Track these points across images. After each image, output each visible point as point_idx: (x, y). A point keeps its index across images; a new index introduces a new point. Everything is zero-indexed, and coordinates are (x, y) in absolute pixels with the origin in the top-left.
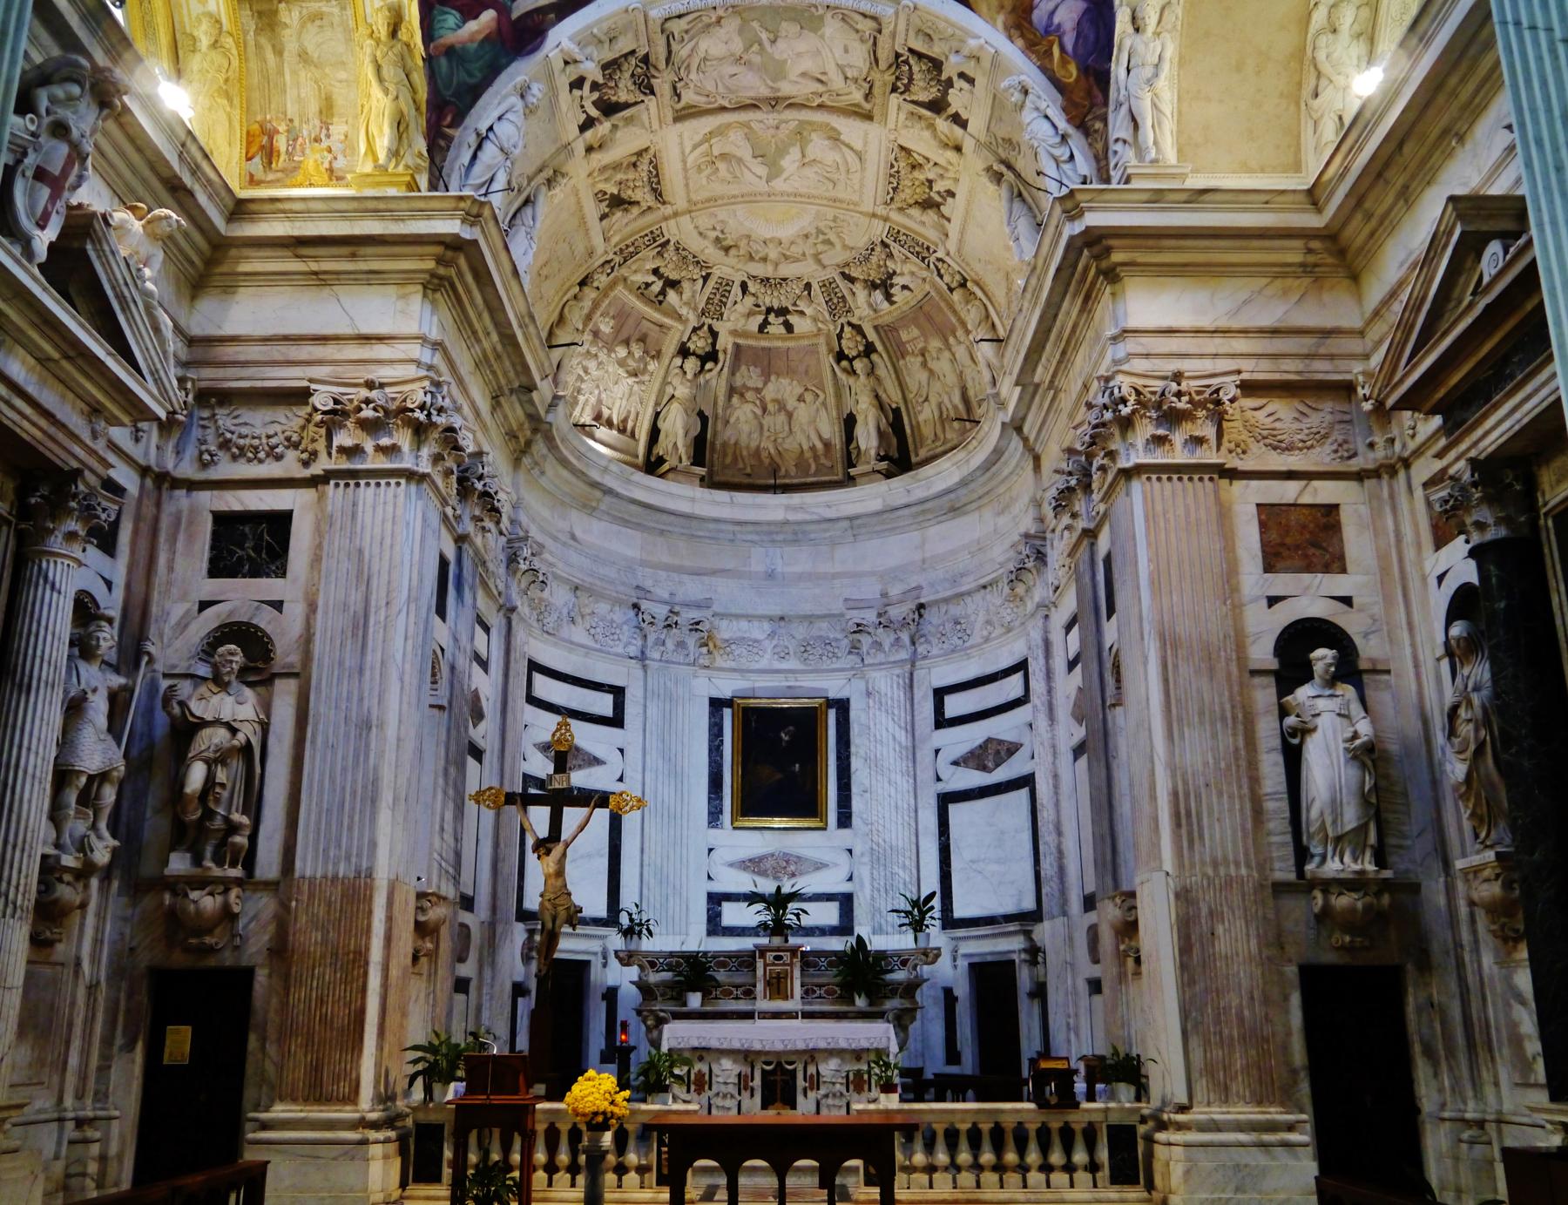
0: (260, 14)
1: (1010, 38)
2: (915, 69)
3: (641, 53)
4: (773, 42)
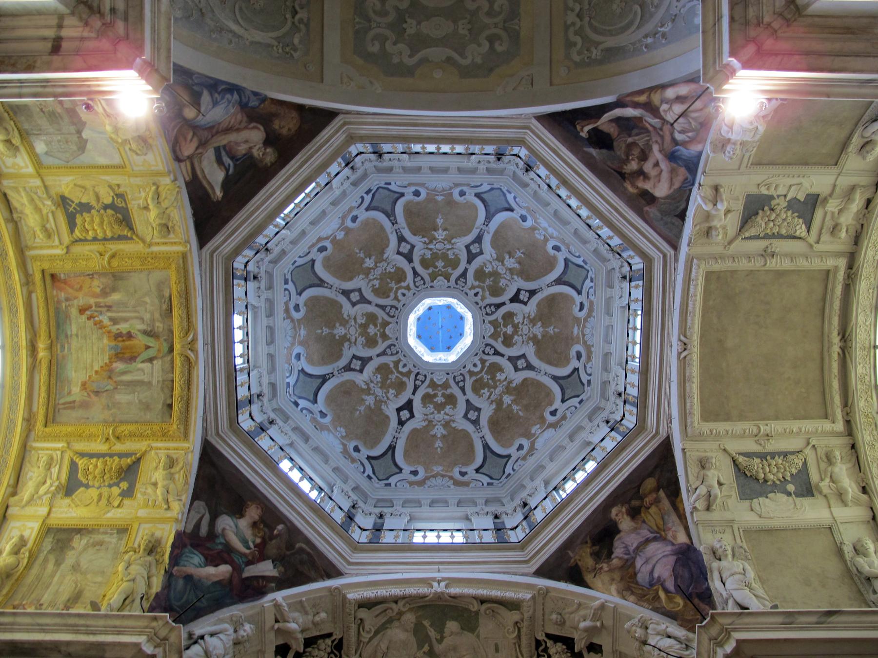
0: (58, 541)
1: (624, 598)
2: (552, 651)
3: (337, 636)
4: (440, 641)
